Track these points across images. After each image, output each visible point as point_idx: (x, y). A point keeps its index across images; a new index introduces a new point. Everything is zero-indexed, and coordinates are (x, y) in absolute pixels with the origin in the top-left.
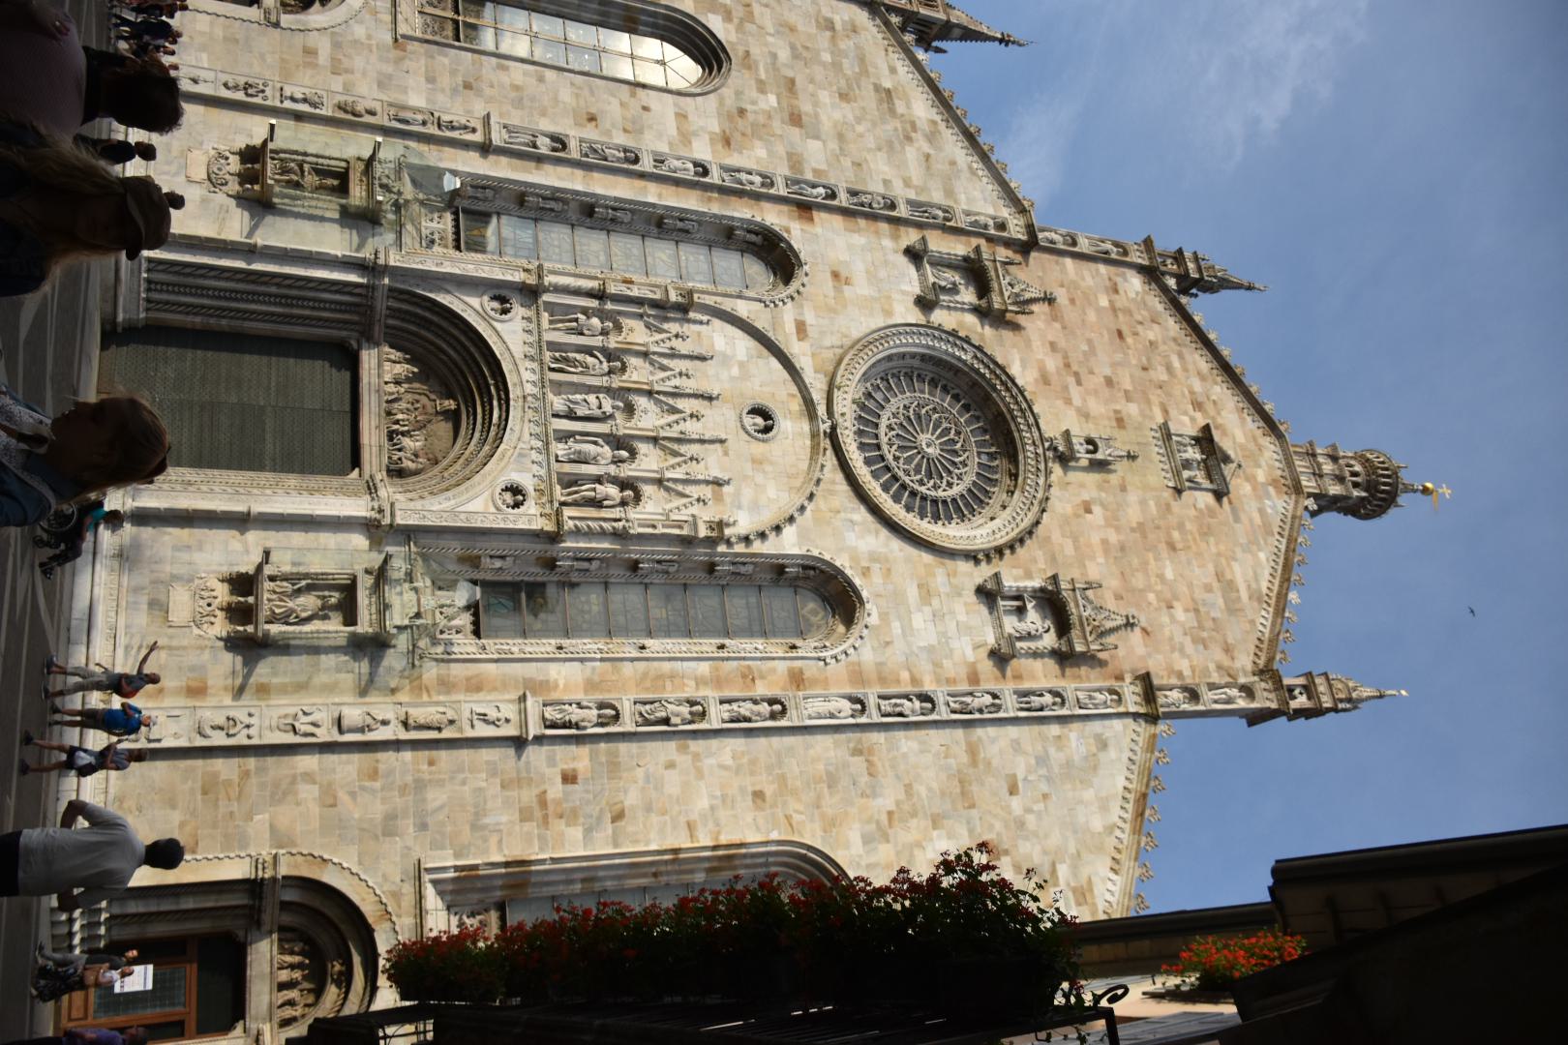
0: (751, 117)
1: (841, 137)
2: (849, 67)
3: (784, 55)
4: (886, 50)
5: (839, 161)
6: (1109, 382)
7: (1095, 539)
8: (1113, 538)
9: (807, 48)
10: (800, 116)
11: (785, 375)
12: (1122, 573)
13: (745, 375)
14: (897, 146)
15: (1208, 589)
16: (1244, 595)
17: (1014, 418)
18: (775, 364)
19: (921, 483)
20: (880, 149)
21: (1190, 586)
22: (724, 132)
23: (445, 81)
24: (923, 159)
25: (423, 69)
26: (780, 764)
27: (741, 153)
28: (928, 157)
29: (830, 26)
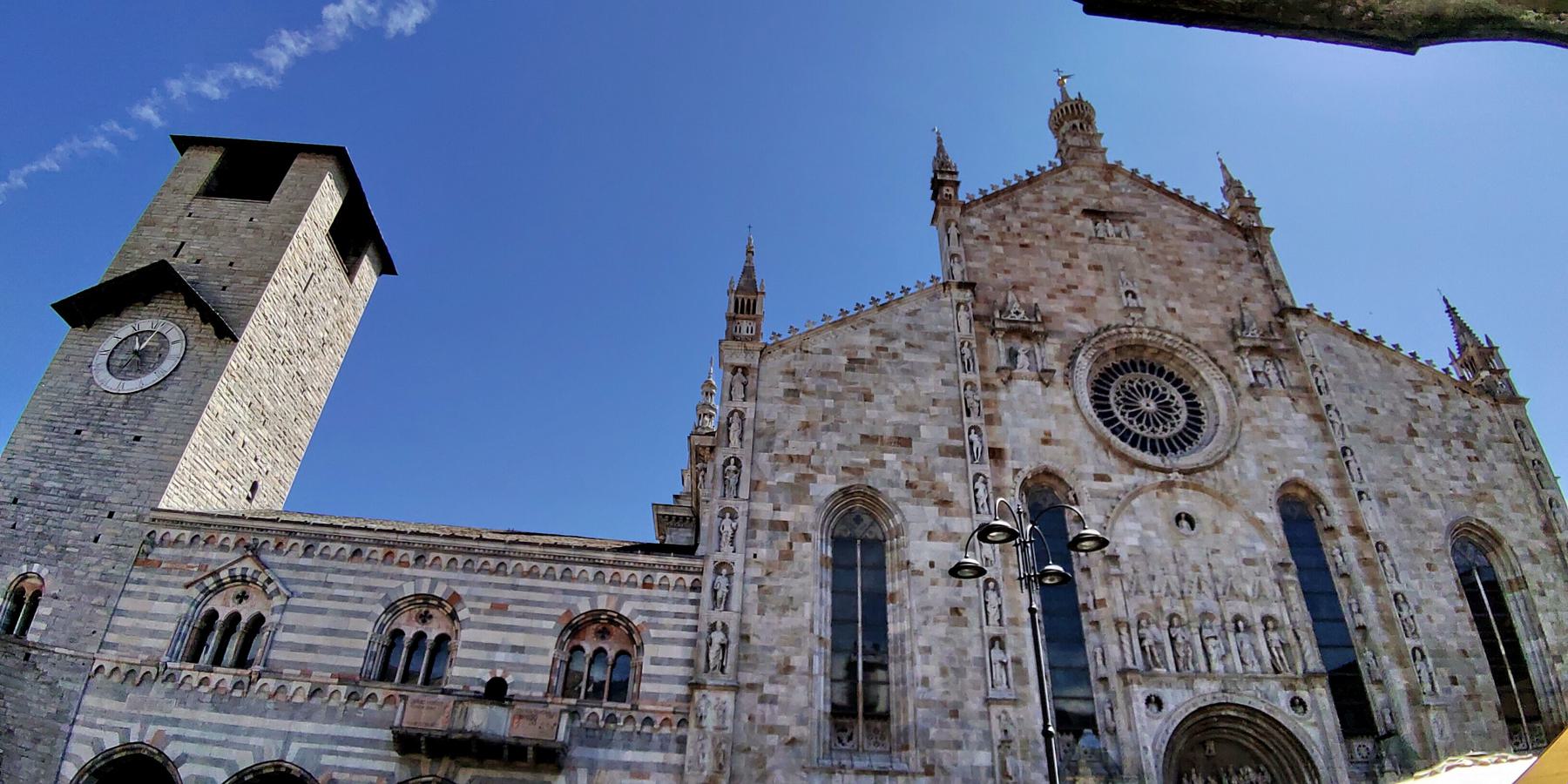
0: (913, 479)
1: (910, 409)
2: (833, 385)
3: (837, 439)
4: (807, 352)
5: (935, 416)
6: (1067, 265)
7: (1193, 312)
8: (1186, 299)
9: (824, 418)
10: (899, 438)
11: (1141, 496)
12: (1211, 302)
13: (1154, 527)
14: (903, 366)
15: (1200, 249)
16: (1195, 228)
17: (1122, 341)
18: (1136, 502)
19: (1177, 417)
20: (913, 381)
21: (1204, 260)
22: (935, 503)
23: (955, 733)
24: (911, 349)
25: (948, 751)
26: (1408, 551)
27: (952, 493)
28: (909, 345)
29: (793, 394)
